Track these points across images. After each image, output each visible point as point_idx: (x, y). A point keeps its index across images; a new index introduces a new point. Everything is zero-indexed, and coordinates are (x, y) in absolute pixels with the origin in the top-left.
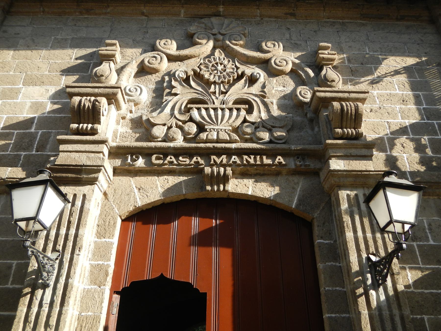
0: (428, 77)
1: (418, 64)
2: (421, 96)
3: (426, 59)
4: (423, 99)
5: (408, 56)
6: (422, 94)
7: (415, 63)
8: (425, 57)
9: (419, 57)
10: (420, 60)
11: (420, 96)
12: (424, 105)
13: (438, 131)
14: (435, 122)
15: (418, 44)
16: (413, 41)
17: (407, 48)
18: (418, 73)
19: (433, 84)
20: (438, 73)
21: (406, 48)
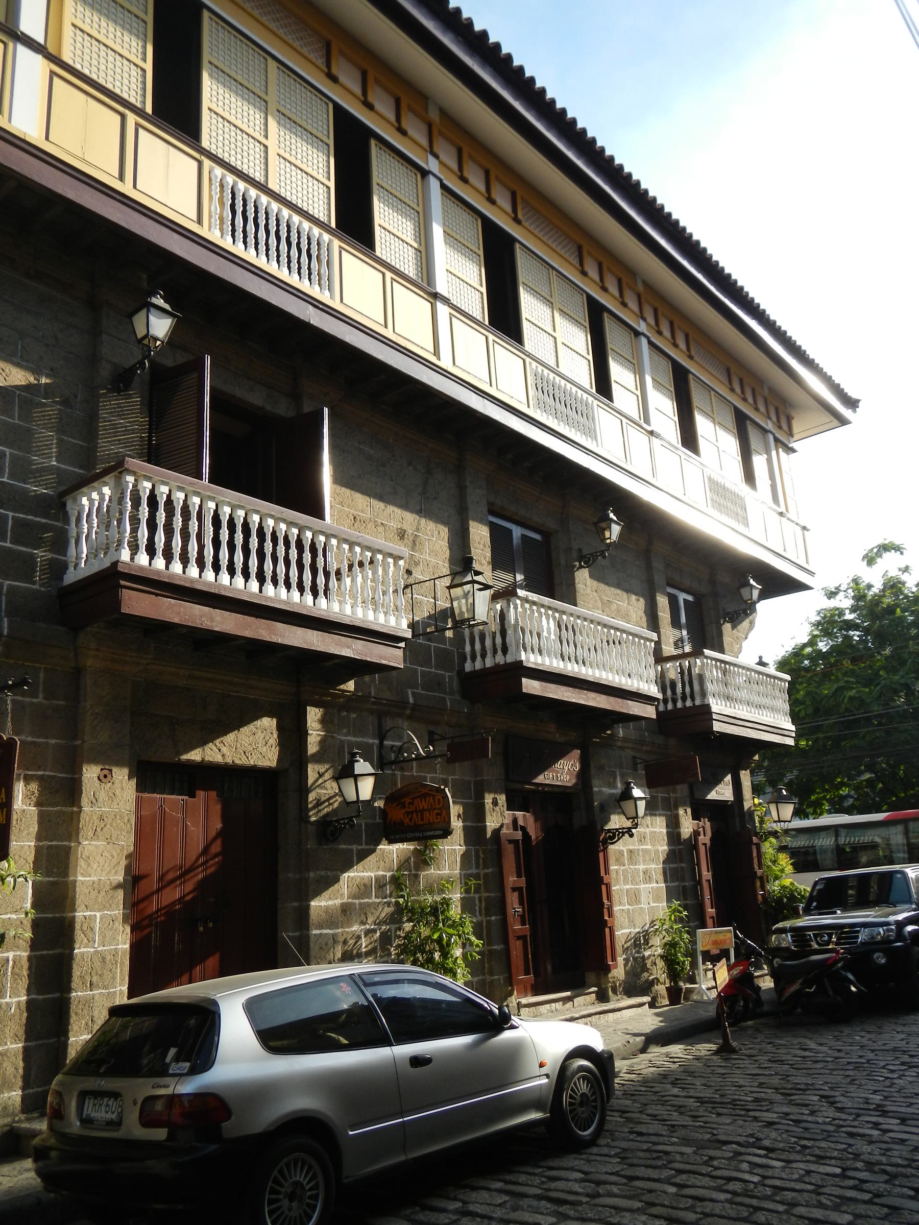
0: (35, 421)
1: (28, 387)
2: (8, 456)
3: (48, 381)
4: (7, 465)
5: (18, 365)
6: (11, 454)
7: (23, 383)
8: (47, 376)
9: (36, 372)
10: (36, 382)
11: (5, 455)
12: (6, 476)
13: (9, 533)
14: (11, 514)
15: (47, 345)
16: (41, 333)
17: (22, 346)
18: (20, 407)
19: (39, 437)
20: (56, 418)
21: (20, 346)
